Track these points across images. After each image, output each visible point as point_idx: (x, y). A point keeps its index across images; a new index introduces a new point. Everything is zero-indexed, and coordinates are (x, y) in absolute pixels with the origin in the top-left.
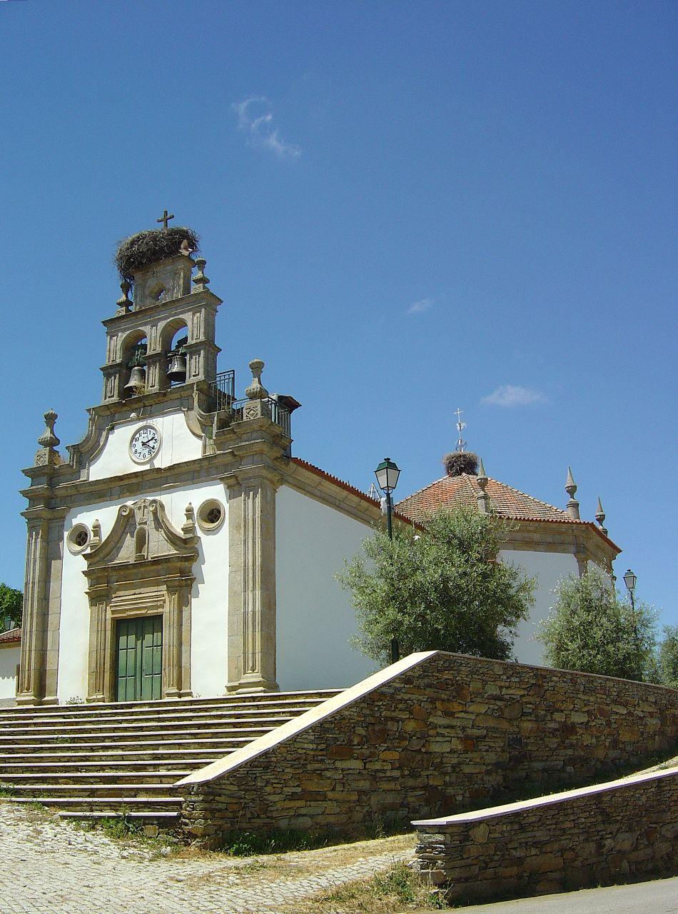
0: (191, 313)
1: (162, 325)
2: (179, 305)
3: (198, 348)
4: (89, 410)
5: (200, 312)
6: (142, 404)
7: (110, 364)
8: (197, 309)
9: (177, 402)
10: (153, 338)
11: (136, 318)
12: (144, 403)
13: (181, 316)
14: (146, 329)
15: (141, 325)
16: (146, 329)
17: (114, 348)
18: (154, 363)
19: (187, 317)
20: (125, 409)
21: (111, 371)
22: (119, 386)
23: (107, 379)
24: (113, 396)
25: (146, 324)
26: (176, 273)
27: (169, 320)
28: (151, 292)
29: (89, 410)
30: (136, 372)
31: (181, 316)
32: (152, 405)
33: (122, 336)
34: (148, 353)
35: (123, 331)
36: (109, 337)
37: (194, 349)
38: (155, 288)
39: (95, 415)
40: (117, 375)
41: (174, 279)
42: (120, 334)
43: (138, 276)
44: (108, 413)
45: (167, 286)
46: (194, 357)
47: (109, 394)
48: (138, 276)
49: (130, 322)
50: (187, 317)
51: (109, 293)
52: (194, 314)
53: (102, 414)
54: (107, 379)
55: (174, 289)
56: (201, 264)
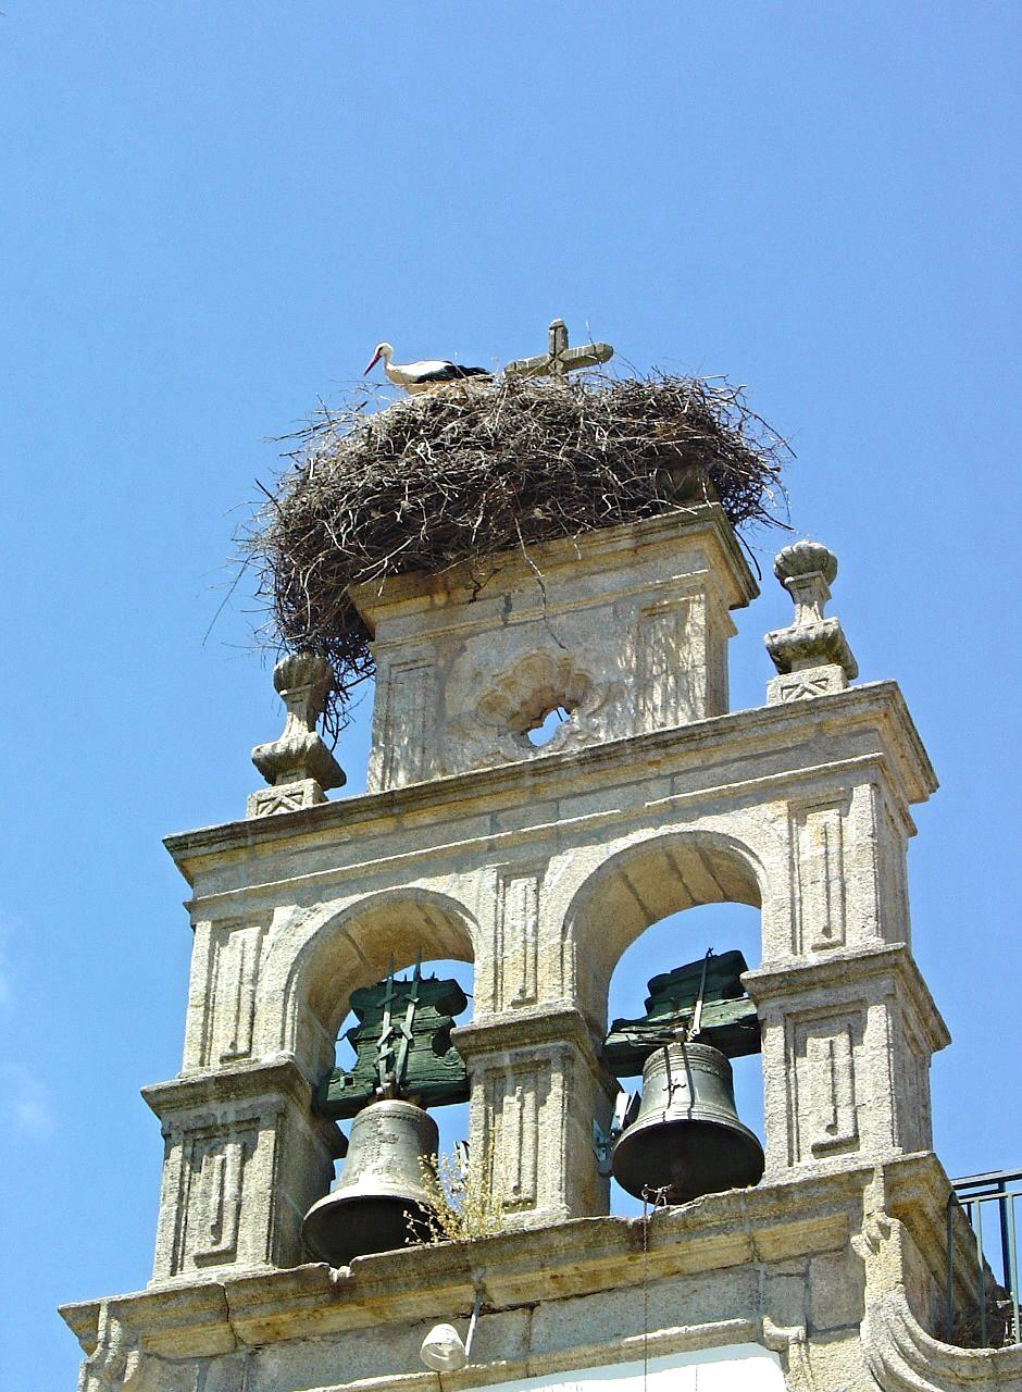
0: (769, 810)
1: (571, 869)
2: (695, 760)
3: (848, 993)
4: (82, 1319)
5: (843, 803)
6: (465, 1293)
7: (215, 1068)
8: (821, 791)
9: (727, 1288)
10: (515, 940)
11: (400, 830)
12: (481, 1291)
13: (708, 823)
14: (472, 889)
15: (429, 867)
16: (472, 889)
17: (244, 992)
18: (531, 1073)
19: (756, 829)
20: (338, 1318)
21: (225, 1111)
22: (276, 1202)
23: (193, 1161)
24: (229, 1255)
25: (462, 862)
26: (657, 612)
27: (620, 844)
28: (492, 705)
29: (82, 1319)
30: (386, 1127)
31: (708, 823)
32: (531, 1307)
33: (295, 927)
34: (476, 1016)
35: (308, 896)
36: (205, 929)
37: (818, 997)
38: (510, 684)
39: (125, 1346)
40: (267, 1138)
41: (640, 642)
42: (282, 914)
43: (398, 622)
44: (211, 1338)
45: (600, 675)
46: (817, 1045)
47: (198, 1244)
48: (398, 622)
49: (347, 851)
50: (756, 829)
51: (217, 706)
52: (798, 814)
53: (168, 1343)
54: (193, 1161)
55: (644, 687)
56: (809, 573)
